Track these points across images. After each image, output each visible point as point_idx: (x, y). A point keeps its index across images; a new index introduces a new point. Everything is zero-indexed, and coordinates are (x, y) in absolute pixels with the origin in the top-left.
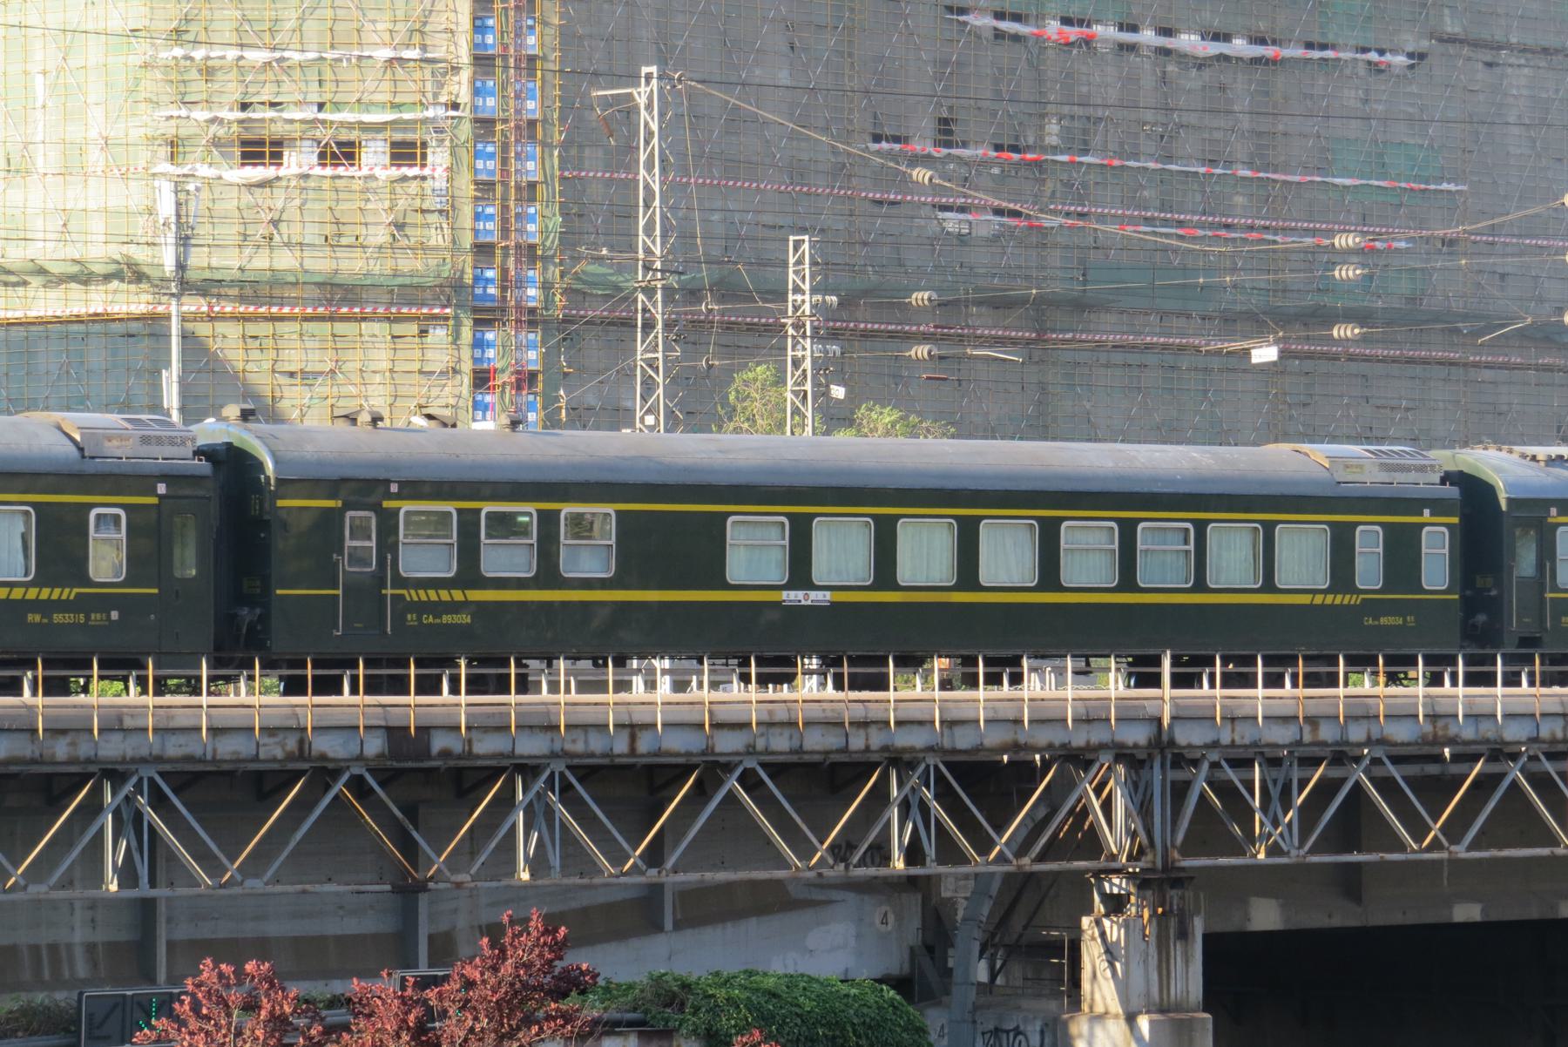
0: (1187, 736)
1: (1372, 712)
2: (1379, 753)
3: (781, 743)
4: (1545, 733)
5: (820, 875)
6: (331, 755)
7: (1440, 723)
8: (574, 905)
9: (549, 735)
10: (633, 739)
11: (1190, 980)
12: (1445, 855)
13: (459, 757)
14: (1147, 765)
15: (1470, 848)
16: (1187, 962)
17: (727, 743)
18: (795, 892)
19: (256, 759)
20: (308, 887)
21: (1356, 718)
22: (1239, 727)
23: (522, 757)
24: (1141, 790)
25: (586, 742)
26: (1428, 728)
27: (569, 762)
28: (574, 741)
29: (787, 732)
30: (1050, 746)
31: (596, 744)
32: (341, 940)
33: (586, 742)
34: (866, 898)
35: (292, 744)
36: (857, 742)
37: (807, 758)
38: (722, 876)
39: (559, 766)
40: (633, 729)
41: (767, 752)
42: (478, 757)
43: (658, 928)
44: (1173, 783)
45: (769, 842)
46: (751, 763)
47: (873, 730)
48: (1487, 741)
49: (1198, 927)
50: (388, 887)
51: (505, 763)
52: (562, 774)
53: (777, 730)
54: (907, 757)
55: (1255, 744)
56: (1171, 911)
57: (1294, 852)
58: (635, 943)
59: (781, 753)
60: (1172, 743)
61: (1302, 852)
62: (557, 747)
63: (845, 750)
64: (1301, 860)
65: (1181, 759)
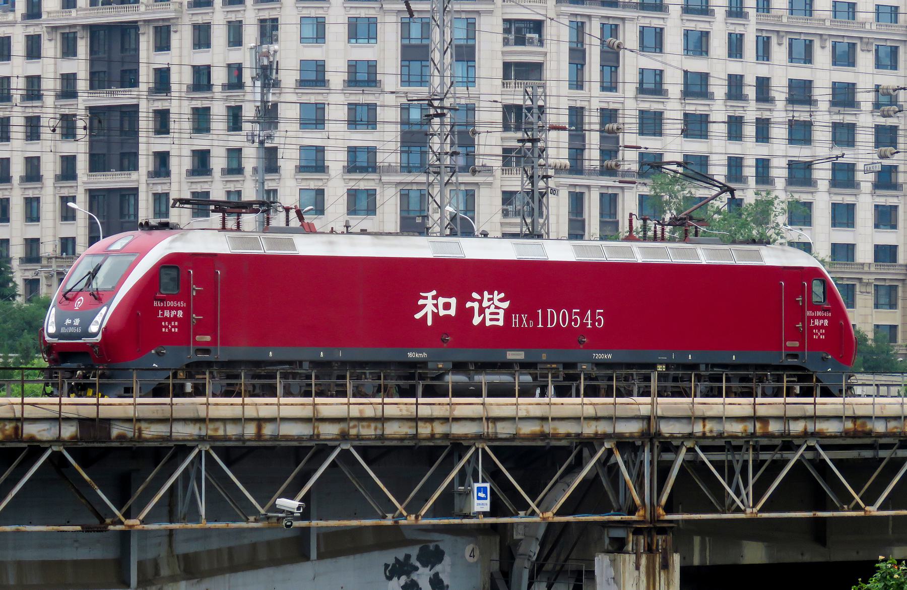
0: (667, 429)
1: (808, 414)
2: (812, 442)
3: (368, 431)
5: (396, 522)
6: (38, 437)
7: (859, 422)
8: (246, 541)
9: (198, 426)
10: (259, 428)
12: (862, 513)
13: (131, 440)
14: (641, 450)
15: (881, 508)
17: (329, 431)
18: (409, 535)
20: (22, 528)
21: (796, 419)
22: (709, 426)
23: (178, 440)
24: (638, 463)
25: (225, 430)
26: (849, 425)
27: (213, 444)
28: (216, 430)
29: (373, 425)
30: (568, 435)
31: (232, 430)
32: (76, 564)
33: (225, 430)
34: (458, 538)
35: (9, 427)
36: (425, 430)
37: (387, 443)
38: (354, 523)
40: (260, 422)
41: (358, 437)
42: (147, 440)
43: (306, 557)
44: (658, 462)
45: (390, 500)
46: (346, 446)
49: (676, 560)
50: (79, 528)
51: (171, 444)
52: (207, 452)
53: (365, 424)
54: (465, 443)
55: (720, 436)
56: (658, 550)
57: (749, 510)
58: (289, 568)
59: (369, 439)
60: (659, 434)
61: (755, 510)
62: (203, 433)
63: (415, 437)
64: (753, 516)
65: (668, 445)
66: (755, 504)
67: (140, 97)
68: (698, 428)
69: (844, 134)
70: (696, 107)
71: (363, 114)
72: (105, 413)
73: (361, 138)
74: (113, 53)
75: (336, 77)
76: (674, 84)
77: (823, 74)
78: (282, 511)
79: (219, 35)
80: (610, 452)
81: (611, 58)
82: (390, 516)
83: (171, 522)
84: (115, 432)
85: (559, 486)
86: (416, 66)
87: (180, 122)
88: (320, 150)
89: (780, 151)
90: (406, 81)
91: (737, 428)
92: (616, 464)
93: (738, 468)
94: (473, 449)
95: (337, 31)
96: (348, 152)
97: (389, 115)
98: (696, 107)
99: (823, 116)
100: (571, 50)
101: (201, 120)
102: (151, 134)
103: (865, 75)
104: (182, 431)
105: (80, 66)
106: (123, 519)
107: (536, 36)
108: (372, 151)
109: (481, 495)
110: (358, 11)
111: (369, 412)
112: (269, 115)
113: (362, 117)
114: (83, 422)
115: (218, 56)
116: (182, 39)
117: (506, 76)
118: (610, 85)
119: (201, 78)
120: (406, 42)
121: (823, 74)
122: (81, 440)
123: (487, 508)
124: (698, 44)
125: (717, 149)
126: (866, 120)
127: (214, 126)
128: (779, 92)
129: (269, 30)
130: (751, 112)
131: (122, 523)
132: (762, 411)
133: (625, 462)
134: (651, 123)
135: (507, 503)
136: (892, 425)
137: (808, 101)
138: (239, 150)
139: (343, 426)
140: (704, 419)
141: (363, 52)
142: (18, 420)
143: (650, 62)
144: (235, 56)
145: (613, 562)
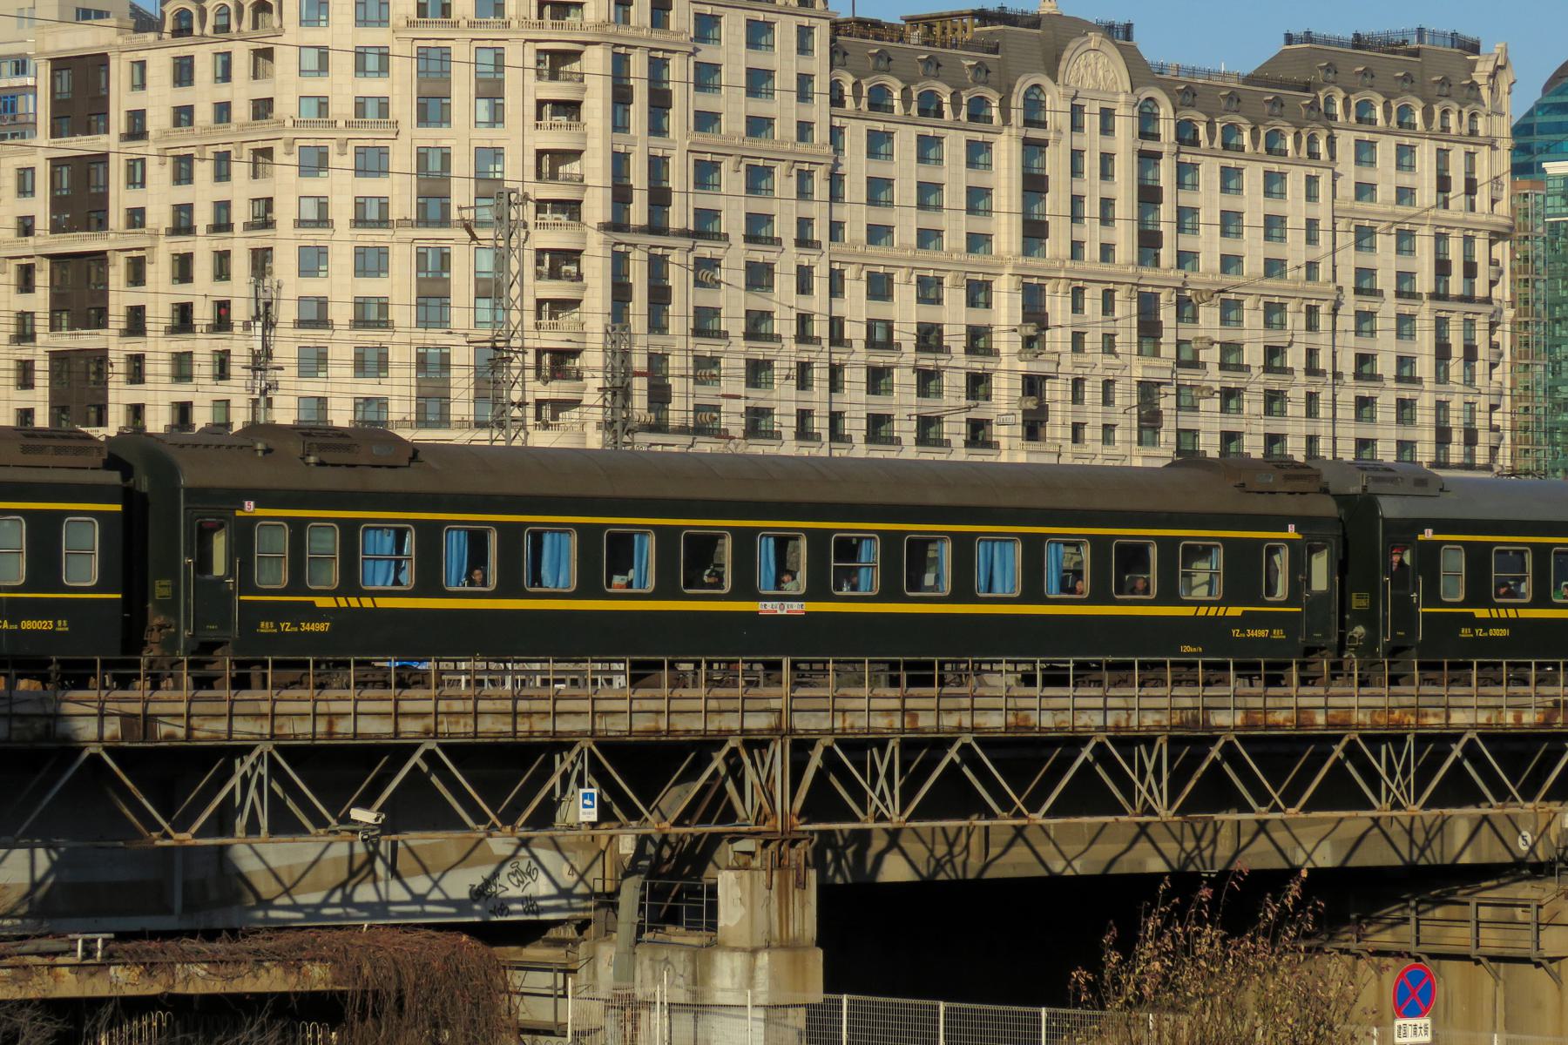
0: (802, 723)
2: (967, 738)
4: (1110, 722)
7: (1021, 714)
10: (331, 724)
11: (806, 919)
16: (803, 907)
17: (410, 727)
19: (9, 740)
21: (950, 711)
26: (1011, 719)
28: (281, 727)
29: (462, 721)
30: (688, 732)
35: (39, 725)
36: (523, 726)
39: (266, 747)
40: (330, 715)
42: (199, 740)
46: (431, 745)
47: (535, 718)
48: (1061, 729)
52: (270, 754)
53: (452, 719)
57: (895, 819)
60: (792, 731)
66: (901, 813)
67: (112, 341)
68: (838, 724)
69: (927, 380)
70: (760, 351)
71: (371, 357)
72: (154, 708)
73: (368, 388)
74: (79, 289)
75: (341, 313)
76: (733, 324)
77: (905, 311)
78: (356, 822)
79: (203, 268)
80: (734, 752)
81: (659, 295)
82: (482, 827)
83: (221, 834)
84: (163, 730)
85: (676, 790)
86: (437, 302)
87: (158, 368)
88: (322, 401)
89: (856, 401)
90: (424, 322)
91: (880, 722)
92: (741, 764)
93: (882, 770)
94: (577, 749)
95: (341, 259)
96: (356, 405)
97: (401, 356)
98: (760, 351)
99: (905, 360)
100: (614, 284)
101: (182, 367)
102: (123, 386)
103: (954, 314)
104: (243, 727)
105: (39, 301)
106: (171, 832)
107: (573, 269)
108: (382, 403)
109: (588, 802)
110: (368, 238)
111: (457, 706)
112: (261, 361)
113: (371, 363)
114: (125, 717)
115: (202, 292)
116: (159, 270)
117: (539, 316)
118: (657, 324)
119: (183, 319)
120: (423, 275)
121: (905, 311)
122: (123, 740)
123: (594, 818)
124: (759, 277)
125: (783, 398)
126: (956, 366)
127: (196, 370)
128: (855, 332)
129: (261, 260)
130: (820, 357)
131: (170, 837)
132: (910, 704)
133: (754, 764)
134: (705, 368)
135: (616, 810)
136: (1060, 717)
137: (889, 344)
138: (228, 401)
139: (430, 721)
140: (844, 711)
141: (371, 287)
142: (49, 716)
143: (706, 298)
144: (221, 291)
145: (739, 879)
